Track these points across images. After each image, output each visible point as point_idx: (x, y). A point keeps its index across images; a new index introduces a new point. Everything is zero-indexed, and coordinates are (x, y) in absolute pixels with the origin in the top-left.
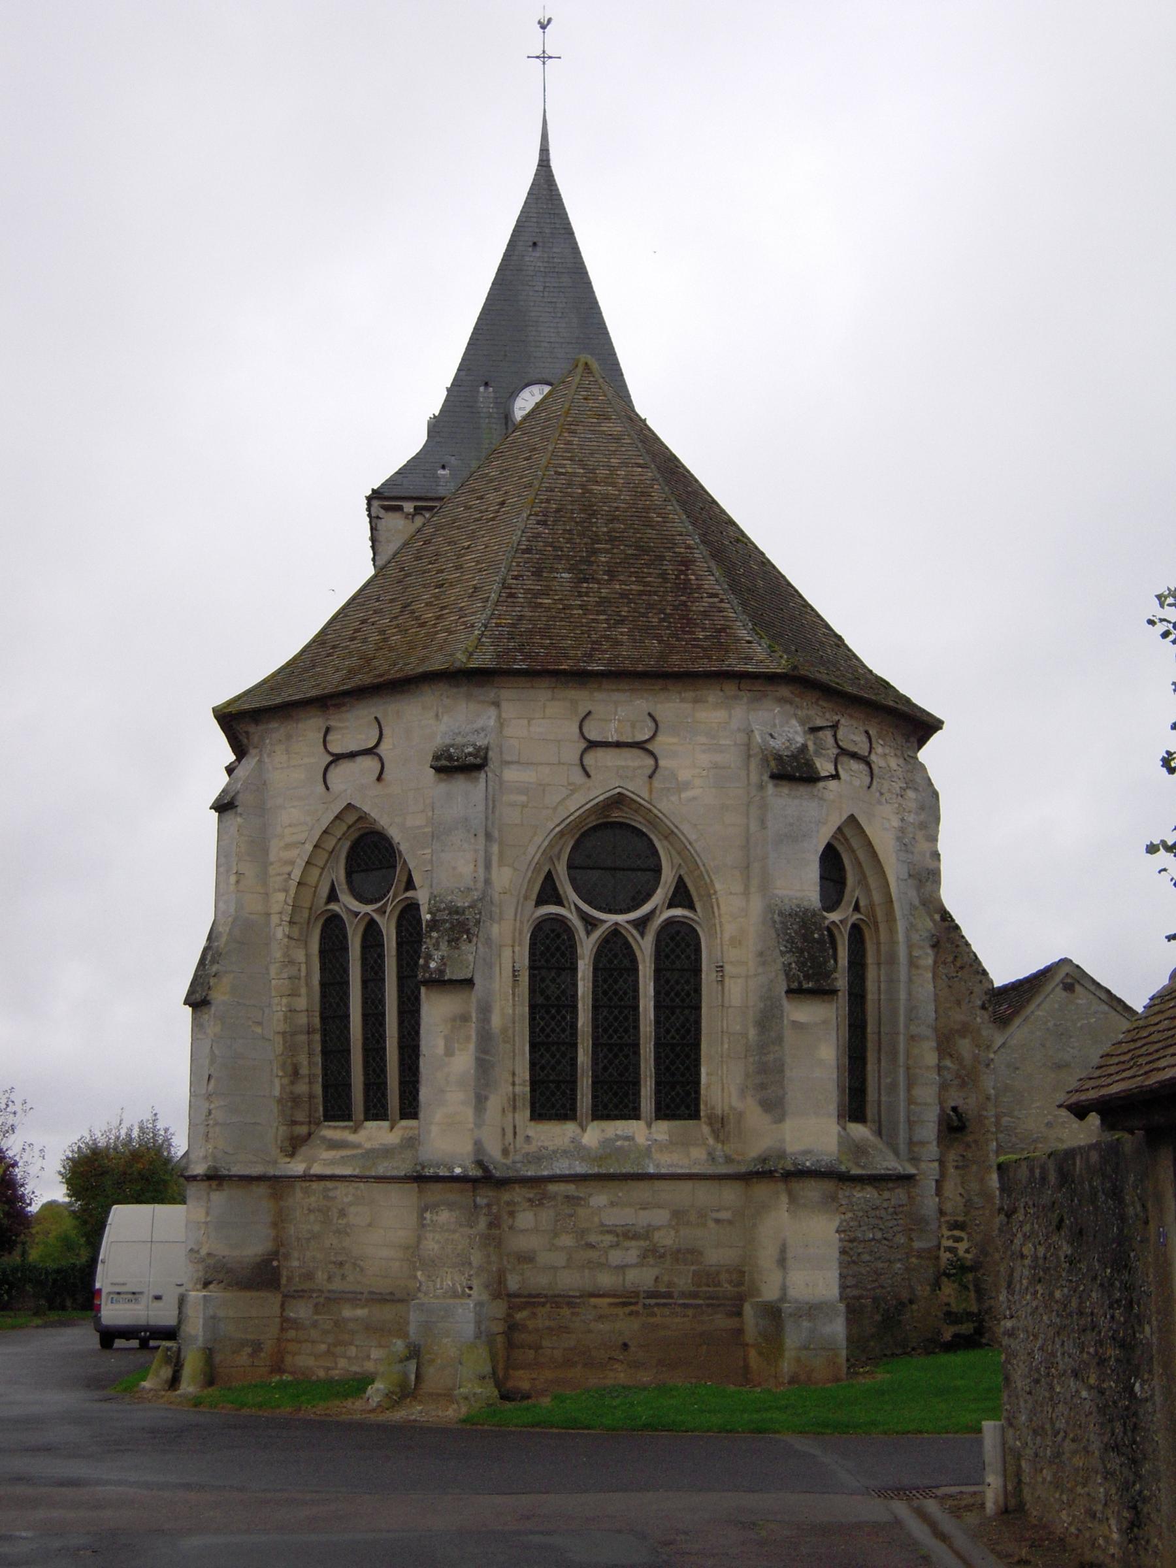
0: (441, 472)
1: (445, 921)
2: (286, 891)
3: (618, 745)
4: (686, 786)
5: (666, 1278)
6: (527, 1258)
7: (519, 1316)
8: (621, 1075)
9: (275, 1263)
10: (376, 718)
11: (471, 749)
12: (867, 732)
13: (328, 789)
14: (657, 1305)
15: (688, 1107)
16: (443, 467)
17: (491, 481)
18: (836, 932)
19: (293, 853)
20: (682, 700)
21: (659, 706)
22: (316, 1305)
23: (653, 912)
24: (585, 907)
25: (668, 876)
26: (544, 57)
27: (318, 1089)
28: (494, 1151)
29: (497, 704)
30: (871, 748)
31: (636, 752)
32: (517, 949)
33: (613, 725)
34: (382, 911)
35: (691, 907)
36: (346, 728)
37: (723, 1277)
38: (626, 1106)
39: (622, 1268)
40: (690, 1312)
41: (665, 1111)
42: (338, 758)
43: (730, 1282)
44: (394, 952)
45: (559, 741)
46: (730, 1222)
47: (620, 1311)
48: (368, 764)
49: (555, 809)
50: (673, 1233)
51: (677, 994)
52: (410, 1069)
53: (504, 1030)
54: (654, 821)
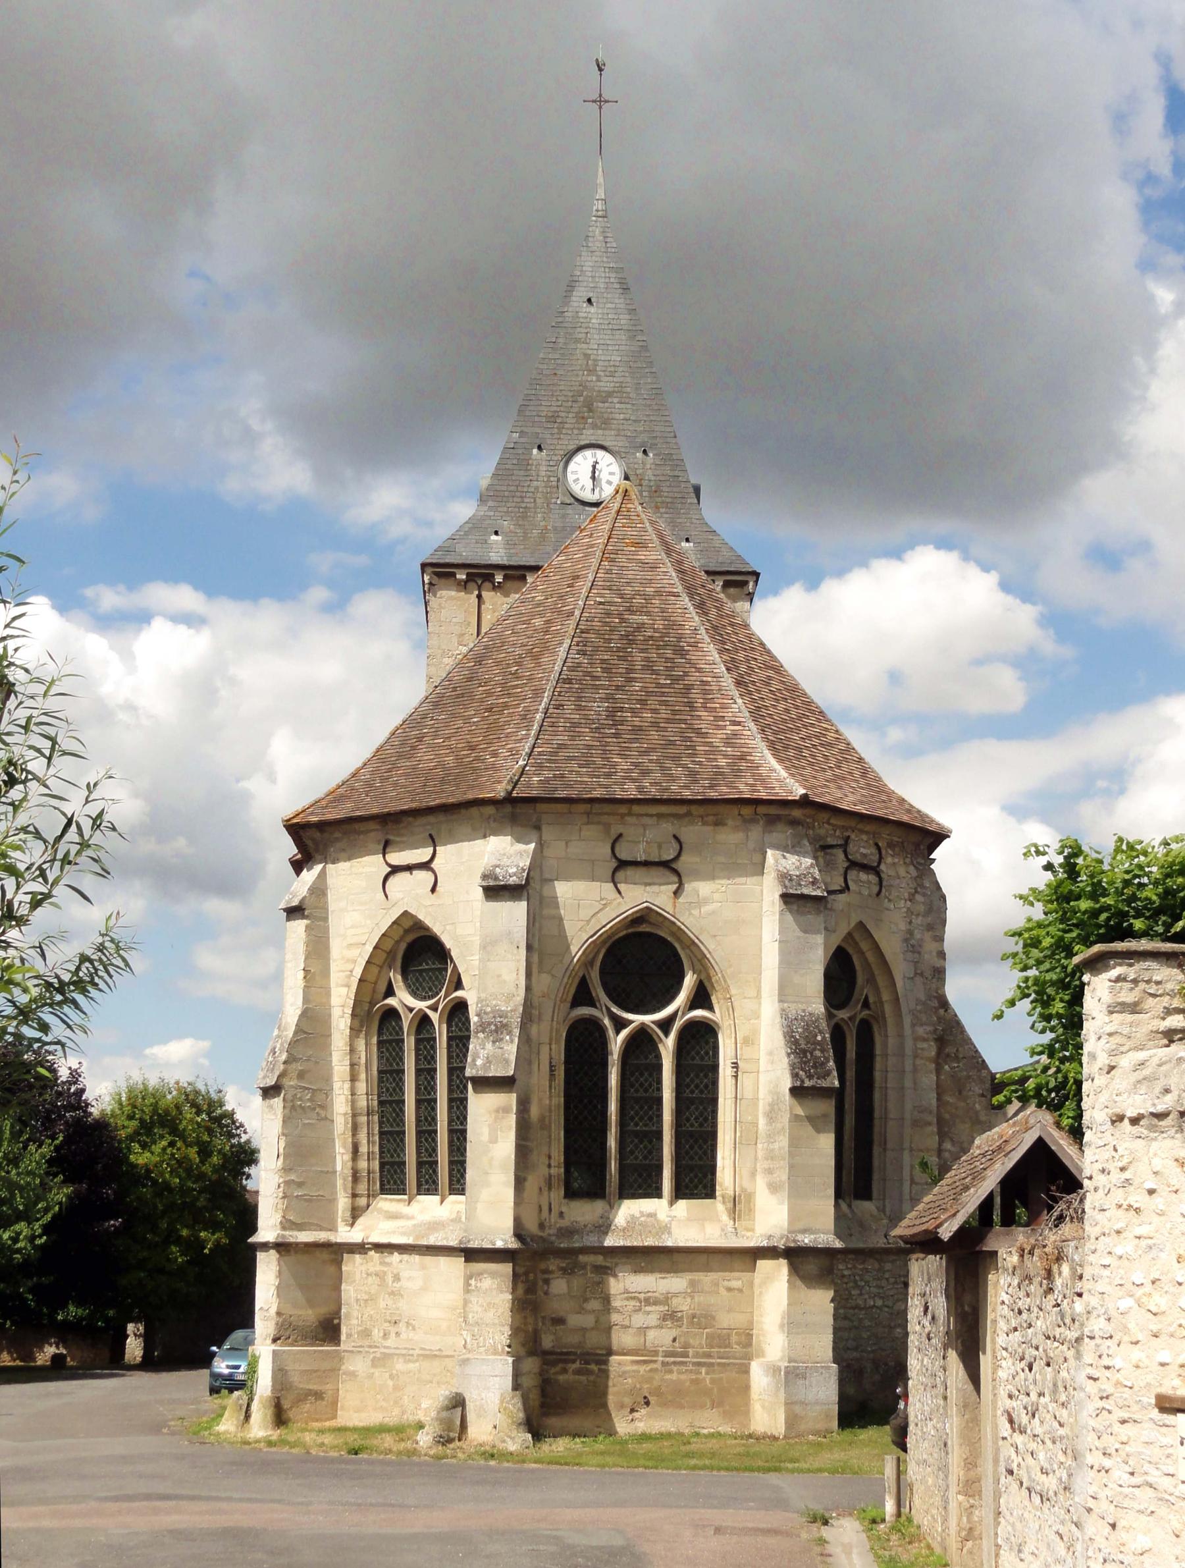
0: (494, 537)
1: (490, 1024)
2: (348, 986)
3: (646, 864)
4: (706, 901)
5: (682, 1339)
6: (559, 1321)
7: (553, 1370)
8: (645, 1158)
9: (336, 1321)
10: (431, 836)
11: (514, 870)
12: (877, 845)
14: (674, 1363)
15: (705, 1187)
16: (496, 533)
17: (539, 605)
18: (845, 1028)
19: (354, 953)
20: (705, 824)
21: (683, 829)
22: (373, 1361)
23: (675, 1014)
24: (615, 1010)
25: (689, 981)
26: (600, 101)
27: (376, 1165)
28: (531, 1226)
29: (538, 828)
30: (881, 858)
31: (662, 871)
32: (553, 1046)
33: (641, 846)
34: (434, 1008)
35: (710, 1008)
37: (734, 1338)
38: (650, 1186)
39: (643, 1330)
40: (703, 1370)
41: (681, 1192)
42: (395, 870)
43: (738, 1344)
44: (445, 1045)
45: (593, 862)
46: (740, 1290)
47: (642, 1369)
48: (424, 876)
49: (588, 921)
50: (689, 1300)
51: (697, 1086)
52: (458, 1149)
53: (542, 1119)
54: (678, 933)
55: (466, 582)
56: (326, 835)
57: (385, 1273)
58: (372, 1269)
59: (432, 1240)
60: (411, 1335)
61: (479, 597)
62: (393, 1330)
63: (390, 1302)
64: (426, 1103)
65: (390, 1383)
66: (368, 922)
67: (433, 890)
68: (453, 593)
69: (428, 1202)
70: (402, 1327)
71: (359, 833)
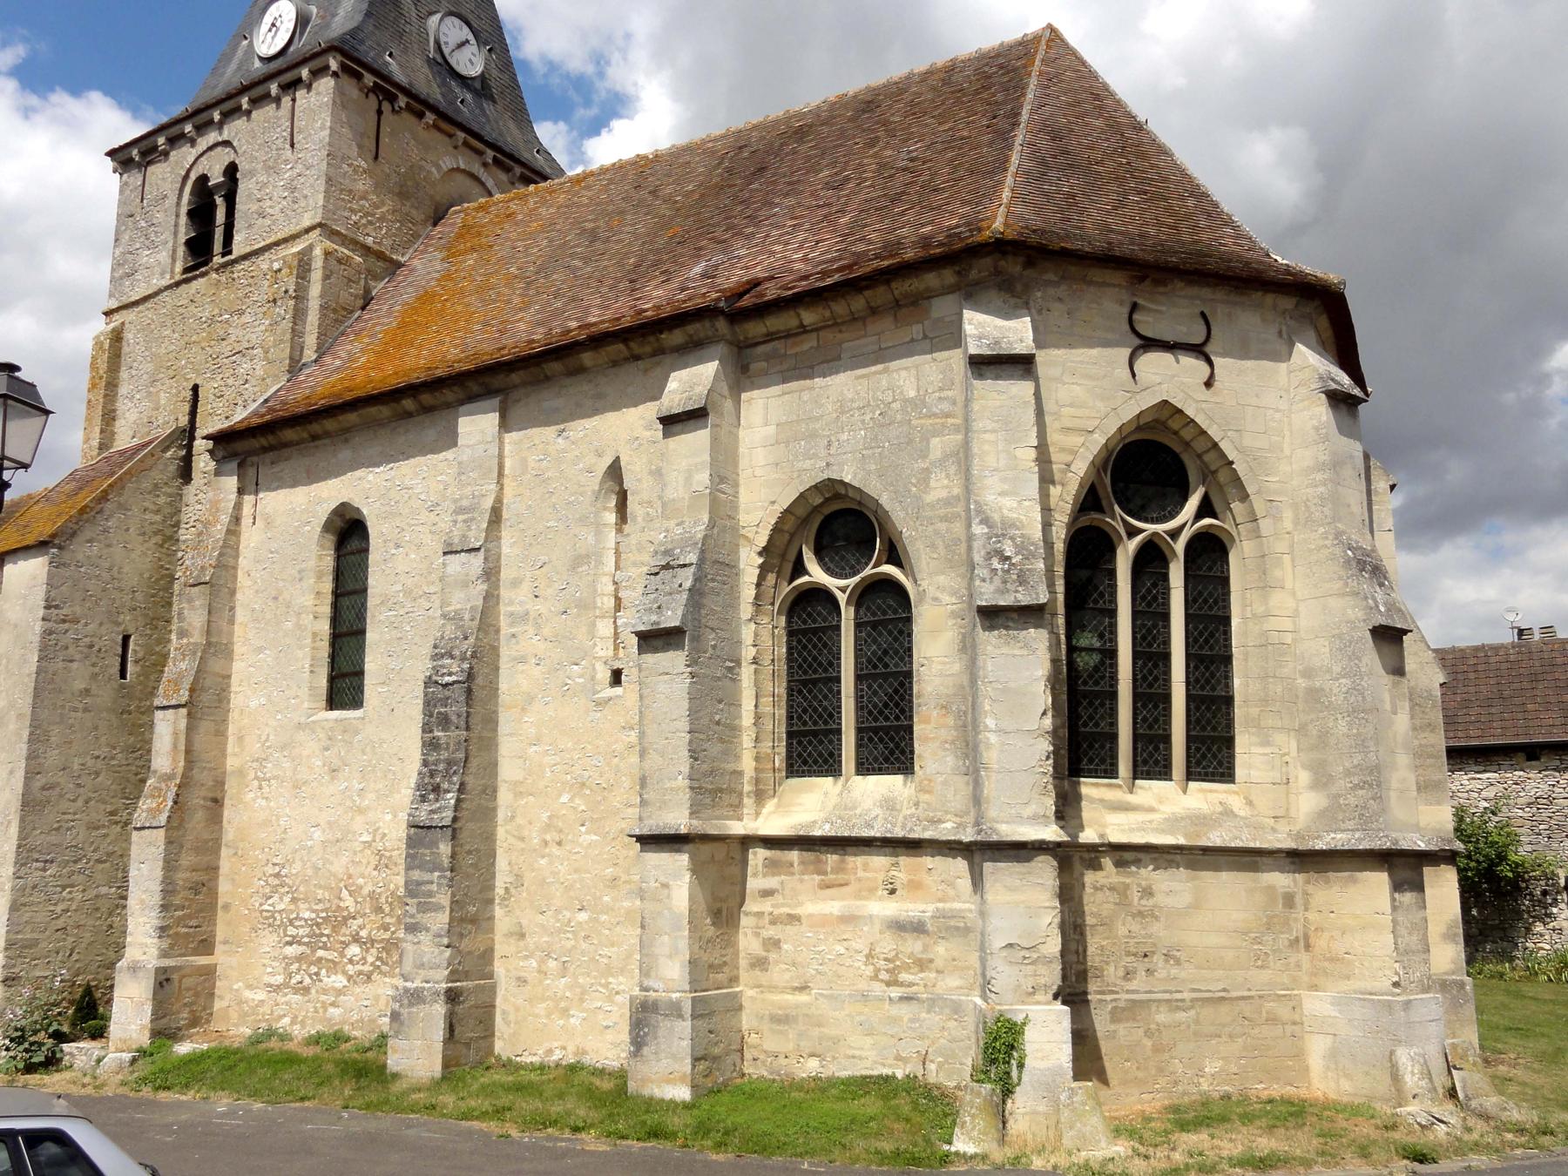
10: (1203, 314)
13: (1134, 375)
36: (1161, 312)
56: (1029, 273)
57: (1127, 887)
58: (1103, 881)
59: (1215, 839)
60: (1174, 971)
61: (380, 112)
62: (1141, 967)
63: (1135, 927)
64: (1152, 657)
65: (1148, 1043)
66: (1099, 404)
67: (1209, 384)
69: (1151, 789)
70: (1158, 959)
71: (1091, 283)
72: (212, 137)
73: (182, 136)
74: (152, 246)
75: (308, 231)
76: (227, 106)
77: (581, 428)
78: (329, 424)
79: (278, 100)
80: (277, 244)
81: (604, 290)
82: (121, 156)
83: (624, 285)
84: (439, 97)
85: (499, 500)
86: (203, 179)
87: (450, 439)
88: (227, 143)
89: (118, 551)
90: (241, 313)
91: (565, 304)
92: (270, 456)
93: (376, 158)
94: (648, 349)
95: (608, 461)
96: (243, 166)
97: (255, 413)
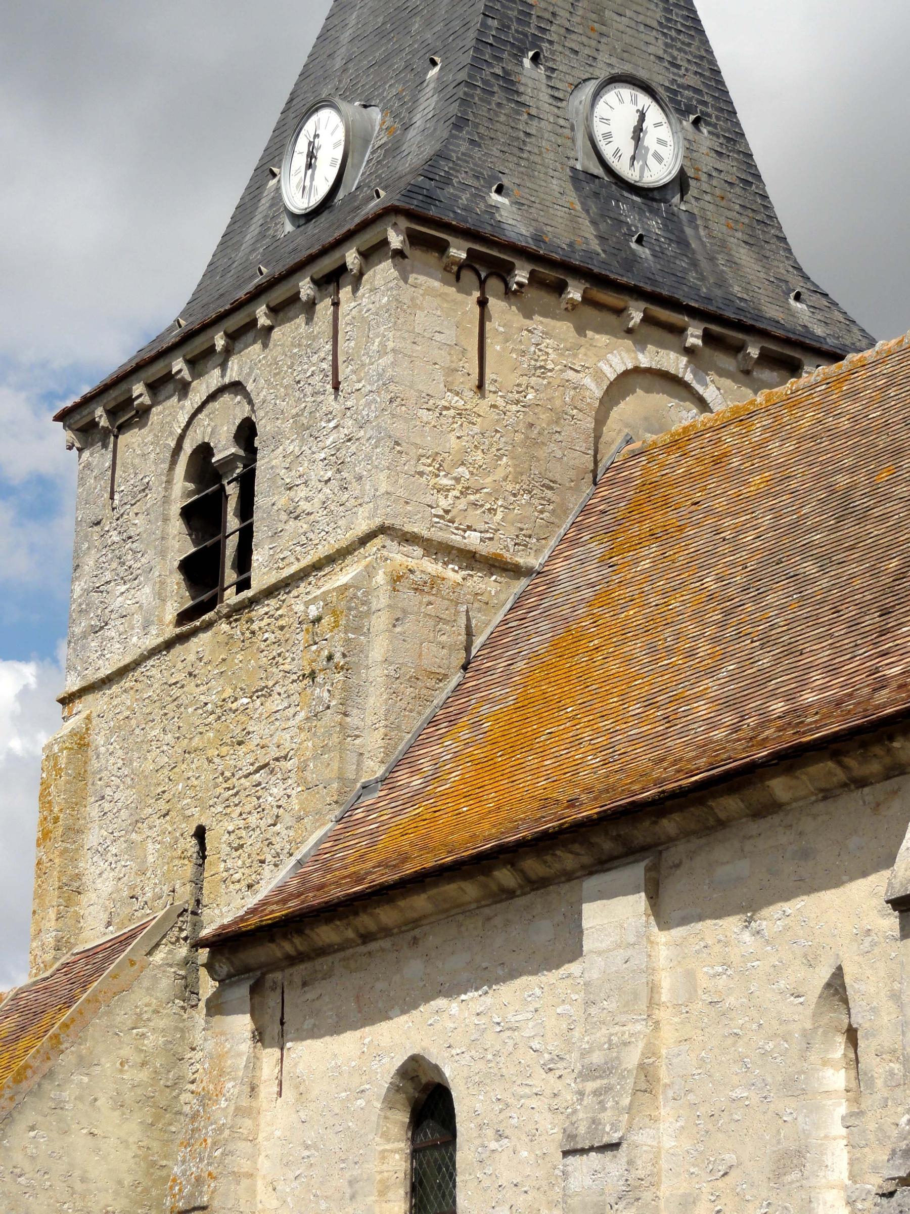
0: (495, 197)
16: (499, 190)
55: (462, 266)
61: (482, 303)
68: (437, 284)
72: (213, 379)
73: (168, 377)
74: (130, 577)
75: (364, 540)
76: (235, 322)
77: (776, 917)
78: (387, 915)
79: (310, 307)
80: (317, 567)
81: (839, 630)
82: (80, 419)
83: (872, 619)
84: (595, 245)
85: (651, 1051)
86: (204, 451)
87: (569, 946)
88: (236, 387)
89: (79, 1139)
90: (265, 693)
91: (777, 661)
92: (300, 971)
93: (480, 386)
94: (875, 767)
95: (825, 974)
96: (264, 427)
97: (281, 894)
